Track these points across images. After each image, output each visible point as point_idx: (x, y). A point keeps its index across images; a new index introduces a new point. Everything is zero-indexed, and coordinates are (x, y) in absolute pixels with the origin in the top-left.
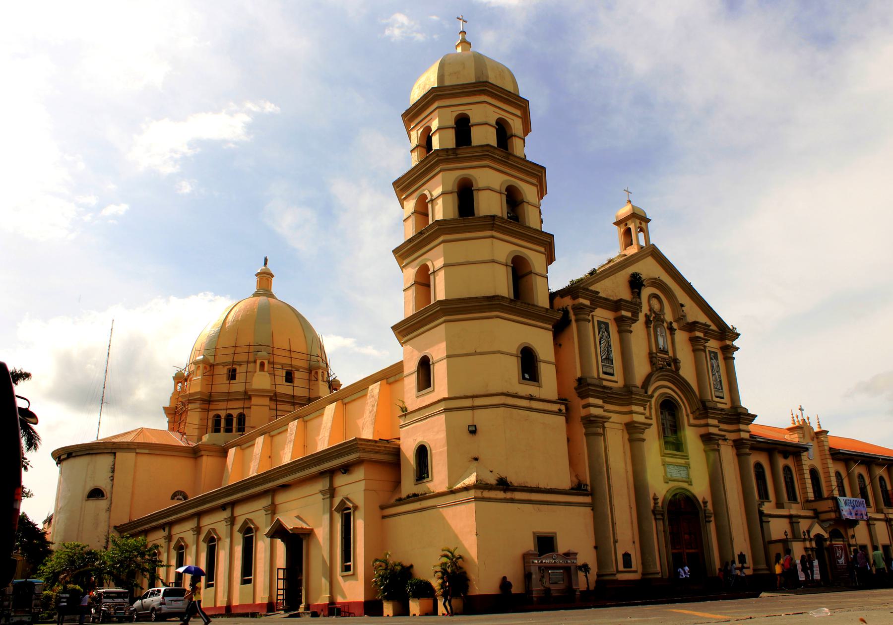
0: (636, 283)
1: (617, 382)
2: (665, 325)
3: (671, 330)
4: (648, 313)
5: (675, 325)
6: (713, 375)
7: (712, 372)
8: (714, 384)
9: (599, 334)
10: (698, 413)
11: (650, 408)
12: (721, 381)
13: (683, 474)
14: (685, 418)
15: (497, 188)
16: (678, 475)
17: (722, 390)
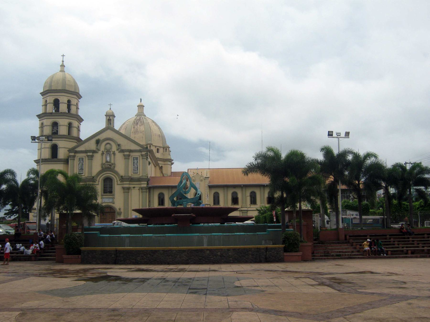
0: (98, 142)
1: (85, 175)
2: (112, 153)
3: (114, 154)
4: (103, 150)
5: (117, 152)
6: (133, 166)
7: (133, 165)
8: (133, 169)
9: (79, 162)
10: (121, 180)
11: (99, 181)
12: (137, 167)
13: (111, 200)
14: (116, 183)
15: (49, 125)
16: (108, 201)
17: (138, 170)
